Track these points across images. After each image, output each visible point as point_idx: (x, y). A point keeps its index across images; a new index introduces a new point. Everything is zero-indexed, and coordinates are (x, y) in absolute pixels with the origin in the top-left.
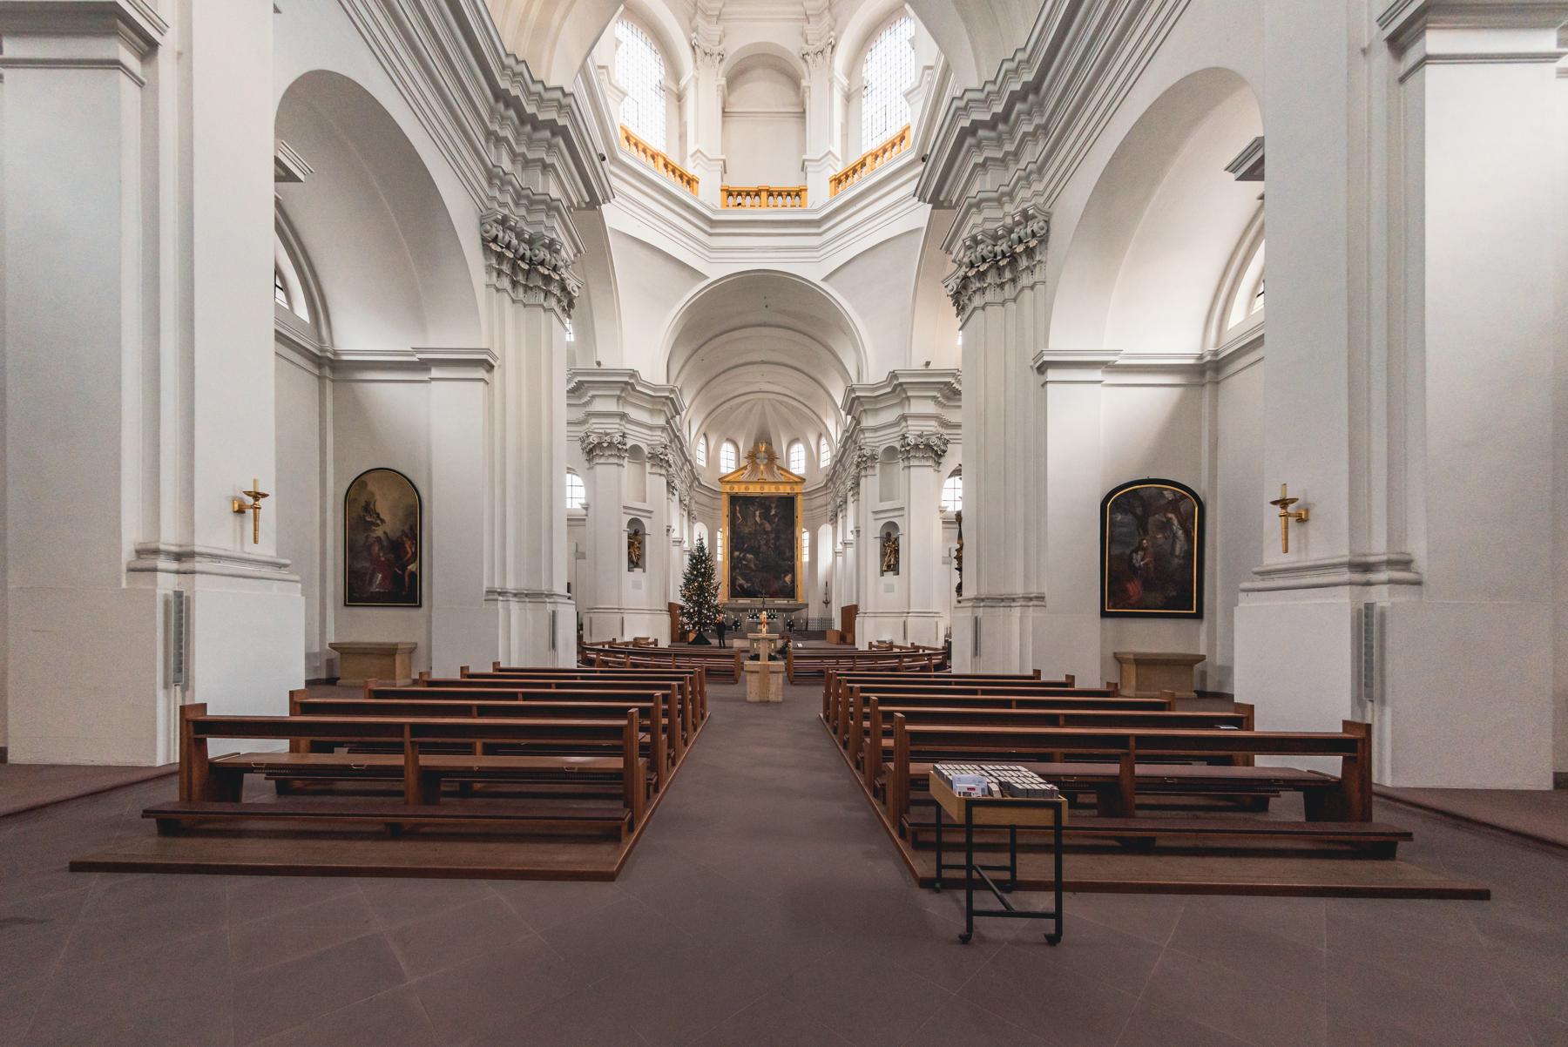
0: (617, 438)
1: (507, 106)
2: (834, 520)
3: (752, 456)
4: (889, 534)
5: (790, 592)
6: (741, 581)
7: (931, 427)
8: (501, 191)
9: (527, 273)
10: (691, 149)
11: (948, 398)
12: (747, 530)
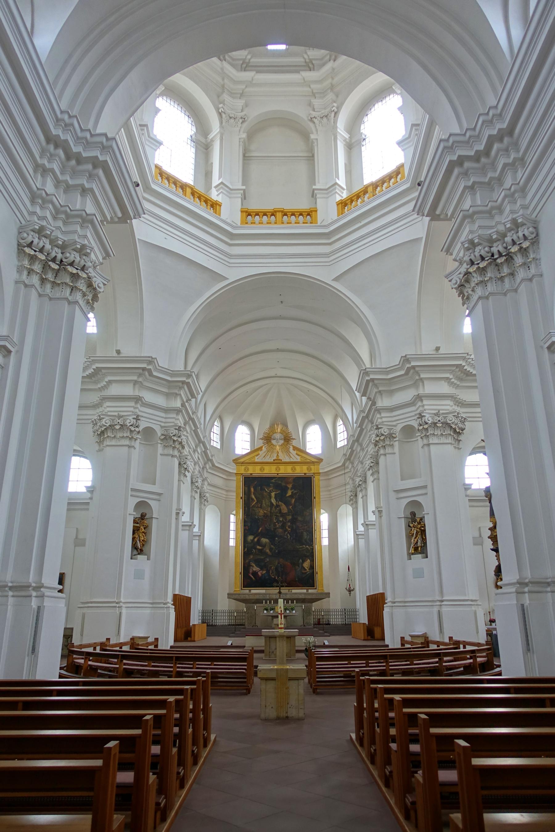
0: (130, 421)
1: (56, 146)
2: (353, 500)
3: (268, 439)
5: (309, 580)
6: (255, 568)
7: (447, 406)
8: (42, 207)
9: (57, 273)
10: (216, 180)
11: (461, 380)
12: (261, 512)
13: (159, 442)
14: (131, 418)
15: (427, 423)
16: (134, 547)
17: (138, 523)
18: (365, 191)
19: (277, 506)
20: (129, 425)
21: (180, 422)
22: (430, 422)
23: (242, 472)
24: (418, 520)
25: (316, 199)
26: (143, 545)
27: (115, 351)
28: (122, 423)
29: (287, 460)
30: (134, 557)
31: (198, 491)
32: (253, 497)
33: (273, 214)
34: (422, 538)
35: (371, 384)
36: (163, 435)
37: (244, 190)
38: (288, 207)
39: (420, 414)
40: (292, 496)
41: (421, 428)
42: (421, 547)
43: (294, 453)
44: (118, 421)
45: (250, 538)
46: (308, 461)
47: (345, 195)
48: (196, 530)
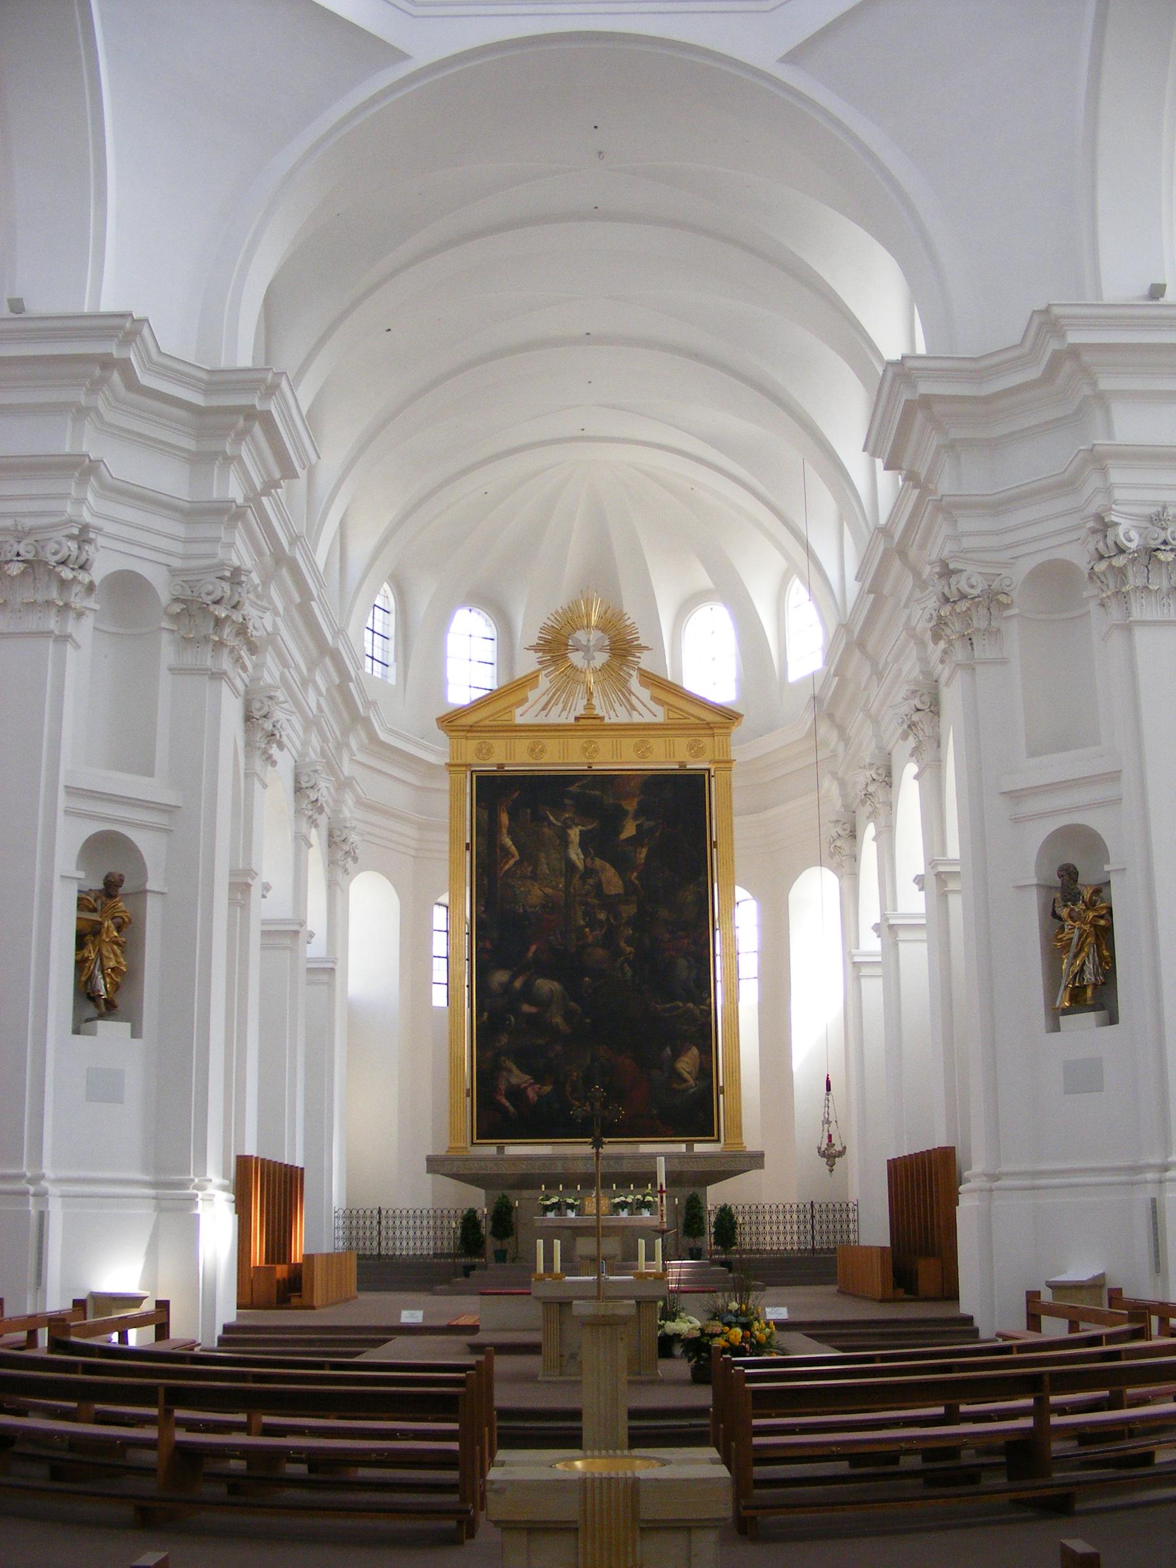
2: (841, 850)
3: (555, 646)
4: (1069, 874)
6: (517, 1077)
12: (536, 894)
13: (165, 625)
14: (59, 535)
15: (1121, 551)
16: (85, 993)
17: (95, 910)
19: (589, 872)
20: (52, 560)
21: (241, 554)
22: (1132, 546)
23: (471, 758)
24: (1087, 895)
26: (117, 987)
27: (6, 305)
28: (30, 556)
29: (619, 716)
30: (84, 1026)
31: (323, 820)
32: (508, 842)
34: (1100, 956)
35: (920, 416)
36: (176, 600)
39: (1099, 518)
40: (636, 841)
41: (1101, 566)
42: (1095, 985)
43: (642, 693)
44: (16, 548)
45: (500, 977)
46: (693, 720)
48: (316, 949)
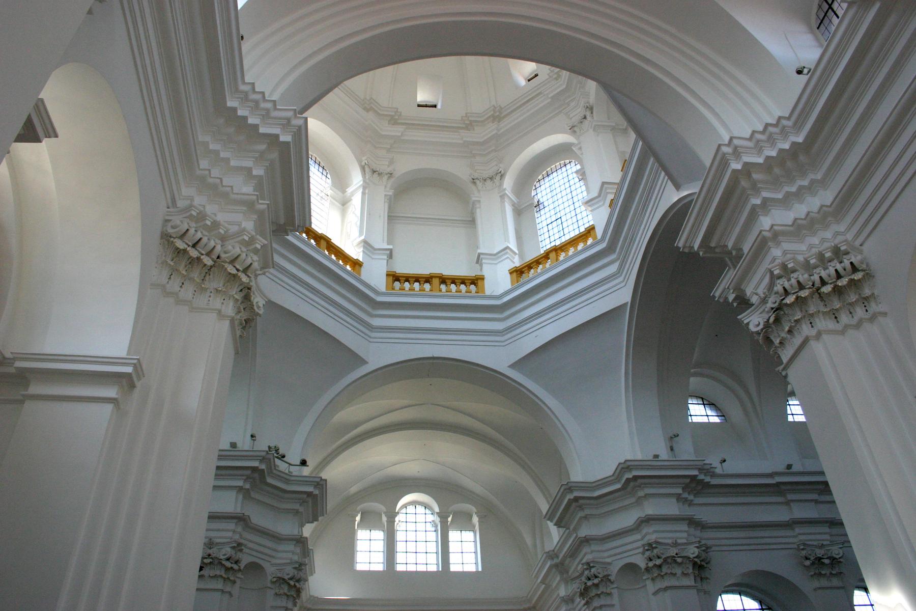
18: (546, 256)
25: (481, 266)
33: (428, 279)
37: (391, 250)
38: (448, 271)
47: (517, 263)
